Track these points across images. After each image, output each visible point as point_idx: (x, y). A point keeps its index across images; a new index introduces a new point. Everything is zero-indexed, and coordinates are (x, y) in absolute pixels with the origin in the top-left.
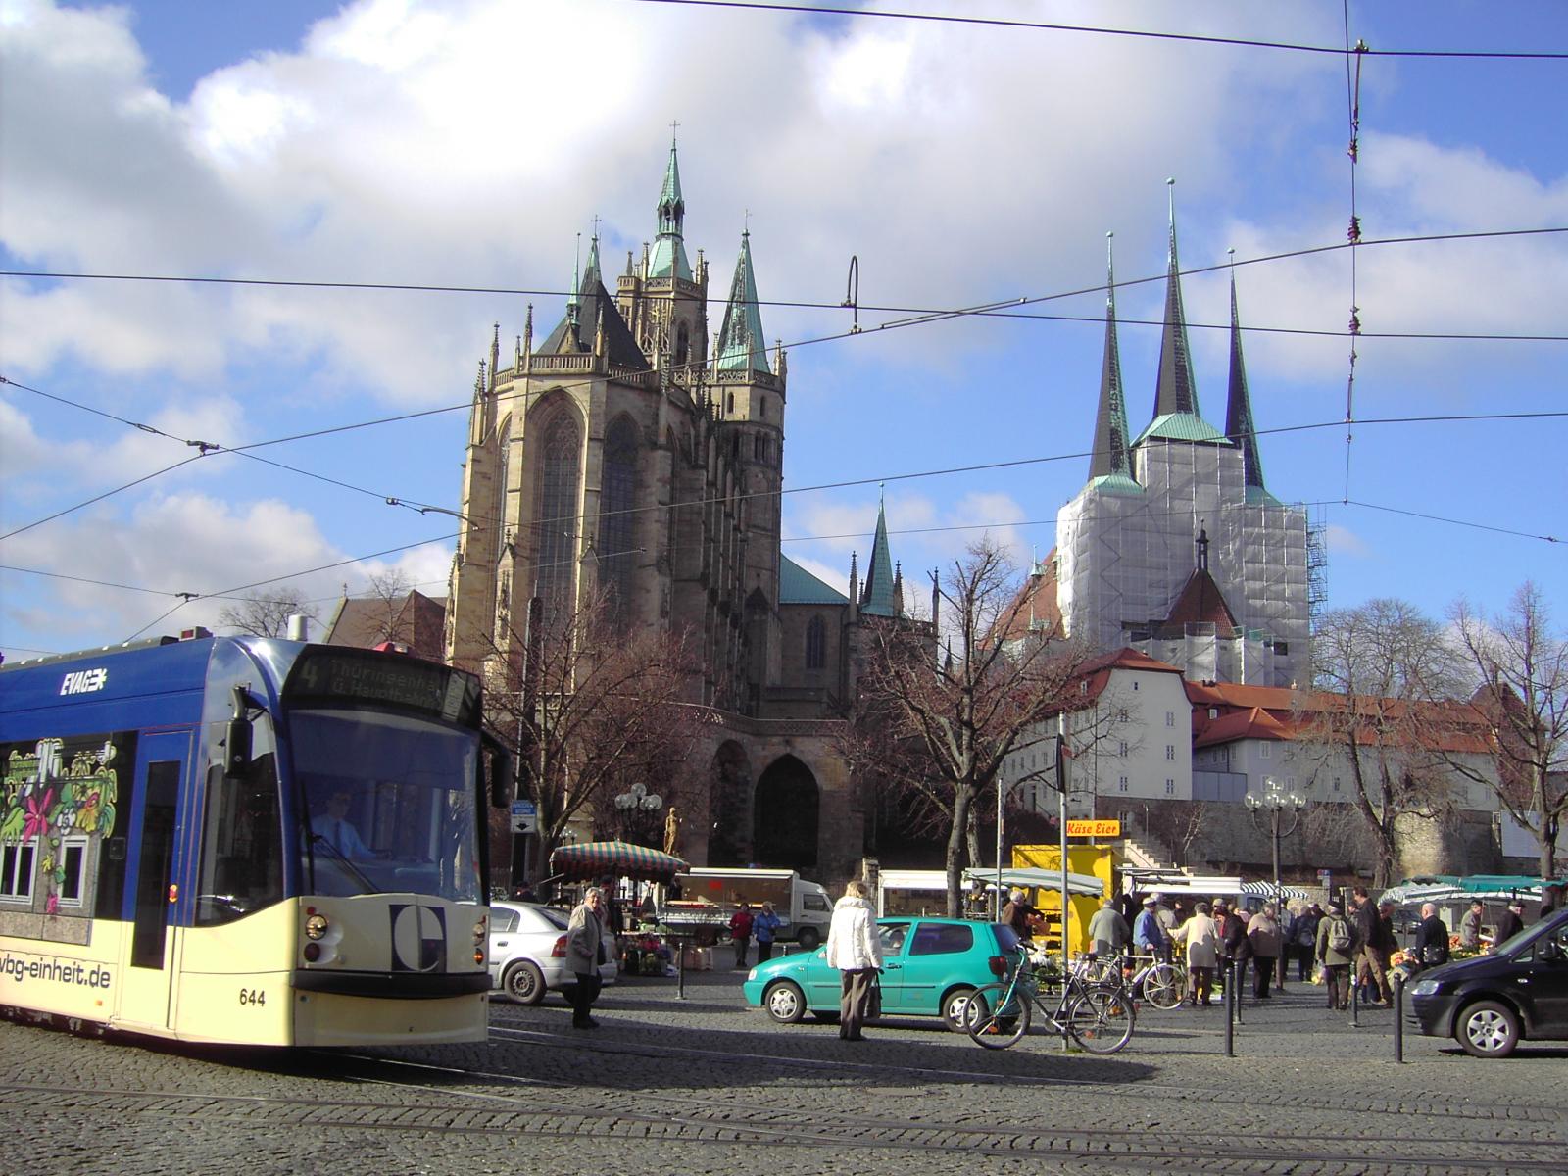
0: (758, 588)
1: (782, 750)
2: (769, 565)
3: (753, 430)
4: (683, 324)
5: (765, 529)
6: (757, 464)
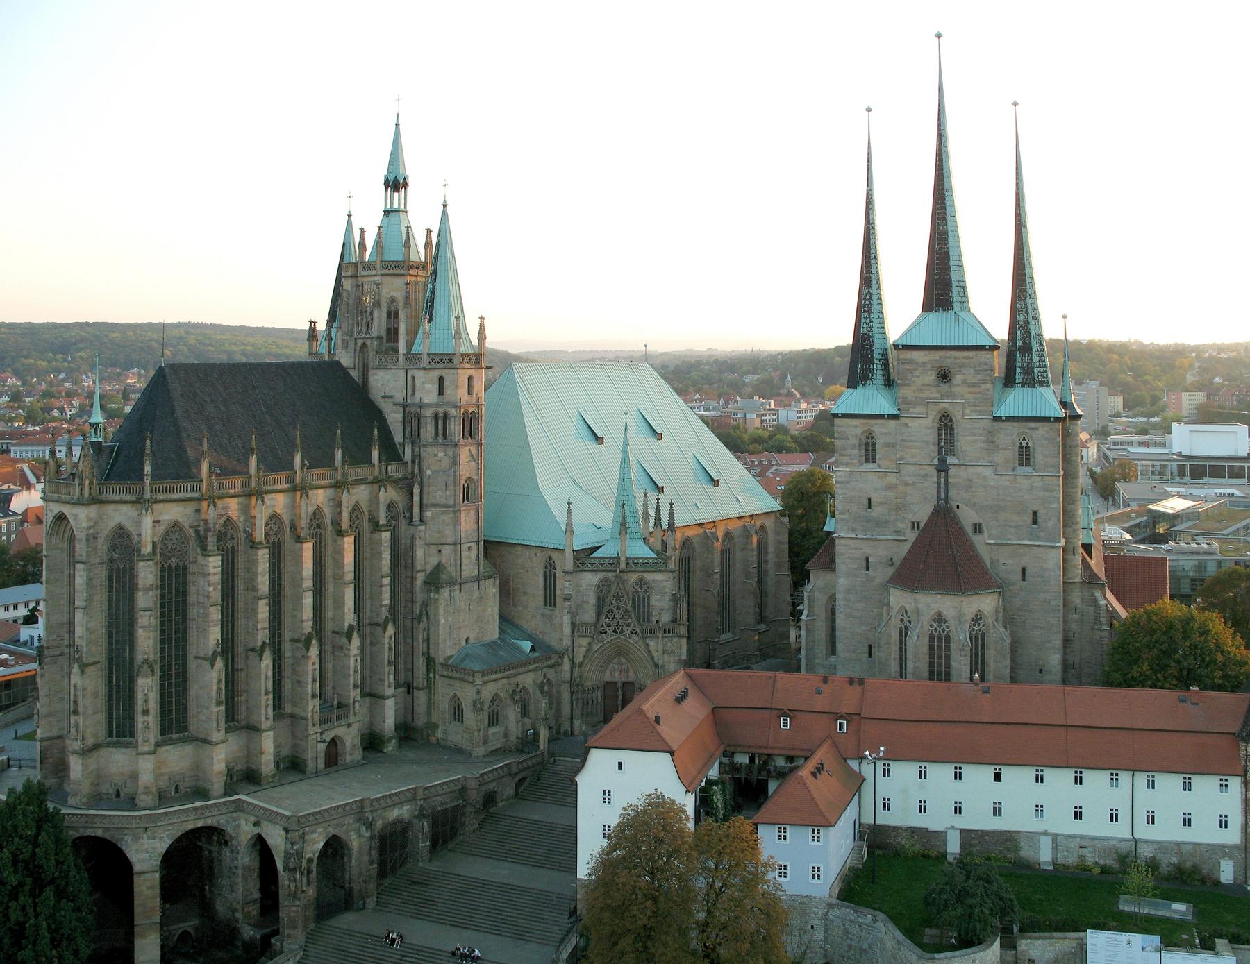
0: (439, 568)
1: (256, 830)
2: (450, 540)
3: (429, 413)
4: (393, 300)
5: (446, 506)
6: (432, 445)
